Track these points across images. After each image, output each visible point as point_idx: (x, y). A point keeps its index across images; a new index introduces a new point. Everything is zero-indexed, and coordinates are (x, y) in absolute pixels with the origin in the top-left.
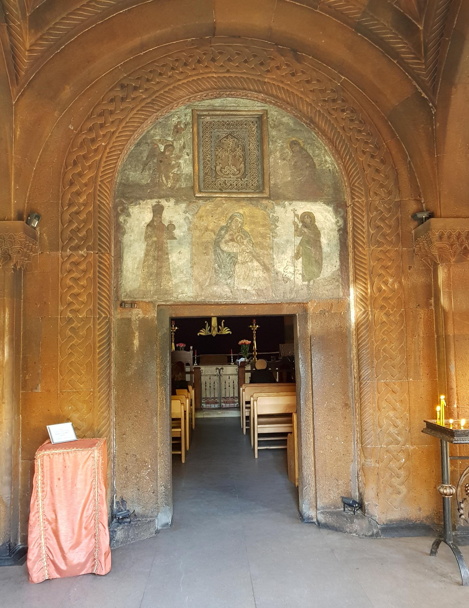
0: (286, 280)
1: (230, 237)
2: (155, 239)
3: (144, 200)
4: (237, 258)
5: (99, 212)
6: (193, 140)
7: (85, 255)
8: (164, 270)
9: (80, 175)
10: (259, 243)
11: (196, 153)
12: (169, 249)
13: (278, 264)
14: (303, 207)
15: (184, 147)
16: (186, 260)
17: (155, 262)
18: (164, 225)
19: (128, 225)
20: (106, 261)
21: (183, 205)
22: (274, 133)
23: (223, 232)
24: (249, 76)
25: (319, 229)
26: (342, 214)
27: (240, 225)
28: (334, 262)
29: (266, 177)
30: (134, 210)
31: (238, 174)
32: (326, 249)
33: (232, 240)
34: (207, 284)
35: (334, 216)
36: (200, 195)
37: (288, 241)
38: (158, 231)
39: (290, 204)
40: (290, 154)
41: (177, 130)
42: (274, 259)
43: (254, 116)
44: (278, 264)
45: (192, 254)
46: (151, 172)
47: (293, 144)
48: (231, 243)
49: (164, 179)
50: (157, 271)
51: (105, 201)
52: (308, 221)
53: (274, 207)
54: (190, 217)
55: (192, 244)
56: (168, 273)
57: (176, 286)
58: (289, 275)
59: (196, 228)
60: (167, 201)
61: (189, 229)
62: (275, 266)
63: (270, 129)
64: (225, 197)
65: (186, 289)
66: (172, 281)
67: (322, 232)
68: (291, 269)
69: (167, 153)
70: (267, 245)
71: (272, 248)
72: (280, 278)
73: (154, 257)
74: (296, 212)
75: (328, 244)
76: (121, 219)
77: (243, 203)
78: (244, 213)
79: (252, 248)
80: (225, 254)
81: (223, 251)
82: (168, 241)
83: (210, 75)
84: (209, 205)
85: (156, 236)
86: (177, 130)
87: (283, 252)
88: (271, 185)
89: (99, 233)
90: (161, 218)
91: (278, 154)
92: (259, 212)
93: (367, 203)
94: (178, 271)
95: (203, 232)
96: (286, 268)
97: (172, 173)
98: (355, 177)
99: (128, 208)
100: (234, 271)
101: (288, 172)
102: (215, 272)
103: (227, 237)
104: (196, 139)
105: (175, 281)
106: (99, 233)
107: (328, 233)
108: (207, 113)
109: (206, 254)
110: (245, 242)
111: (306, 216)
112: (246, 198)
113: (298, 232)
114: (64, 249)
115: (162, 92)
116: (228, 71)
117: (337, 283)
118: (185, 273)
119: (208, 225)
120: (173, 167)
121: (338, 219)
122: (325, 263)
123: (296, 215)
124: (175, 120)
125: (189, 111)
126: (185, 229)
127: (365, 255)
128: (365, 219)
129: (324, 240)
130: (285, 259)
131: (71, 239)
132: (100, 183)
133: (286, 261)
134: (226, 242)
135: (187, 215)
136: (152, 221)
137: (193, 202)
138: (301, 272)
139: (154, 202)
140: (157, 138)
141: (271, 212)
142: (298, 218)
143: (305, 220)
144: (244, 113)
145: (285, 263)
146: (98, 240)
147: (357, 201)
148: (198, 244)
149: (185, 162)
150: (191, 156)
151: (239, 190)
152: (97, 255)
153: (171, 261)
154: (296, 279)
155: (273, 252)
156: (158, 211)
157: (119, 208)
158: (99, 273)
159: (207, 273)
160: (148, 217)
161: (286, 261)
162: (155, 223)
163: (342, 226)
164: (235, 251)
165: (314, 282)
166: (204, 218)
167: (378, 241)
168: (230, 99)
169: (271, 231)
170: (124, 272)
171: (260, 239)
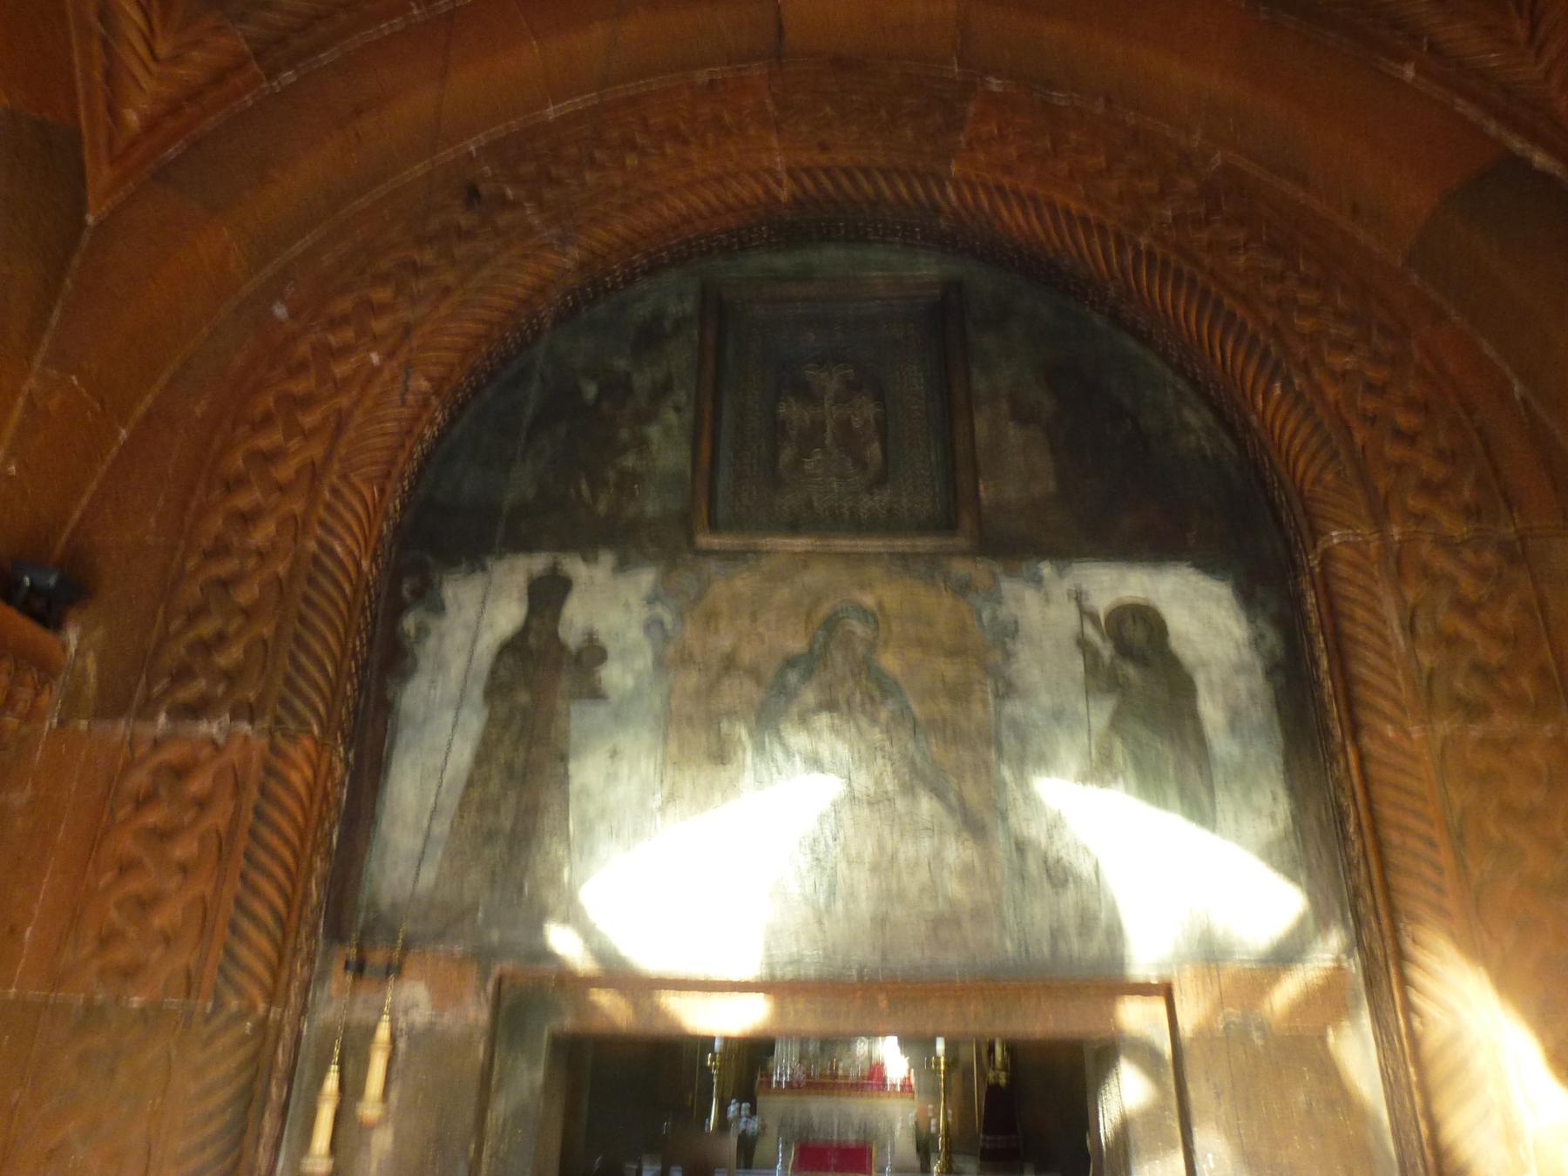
3: (500, 557)
5: (311, 581)
7: (221, 740)
9: (271, 457)
14: (1114, 585)
15: (663, 390)
18: (562, 647)
19: (431, 643)
21: (646, 578)
23: (793, 677)
30: (460, 593)
39: (1061, 575)
41: (650, 338)
49: (584, 487)
52: (1137, 634)
54: (668, 618)
59: (685, 659)
60: (585, 560)
61: (660, 663)
67: (1200, 680)
72: (1033, 867)
76: (409, 623)
77: (875, 572)
78: (880, 605)
82: (575, 709)
91: (1005, 407)
92: (939, 605)
113: (1100, 678)
114: (146, 712)
119: (735, 650)
123: (1087, 614)
131: (182, 675)
135: (659, 610)
136: (523, 633)
139: (539, 563)
146: (279, 681)
150: (689, 415)
151: (860, 526)
153: (574, 786)
160: (508, 615)
162: (532, 640)
170: (384, 825)
171: (945, 706)
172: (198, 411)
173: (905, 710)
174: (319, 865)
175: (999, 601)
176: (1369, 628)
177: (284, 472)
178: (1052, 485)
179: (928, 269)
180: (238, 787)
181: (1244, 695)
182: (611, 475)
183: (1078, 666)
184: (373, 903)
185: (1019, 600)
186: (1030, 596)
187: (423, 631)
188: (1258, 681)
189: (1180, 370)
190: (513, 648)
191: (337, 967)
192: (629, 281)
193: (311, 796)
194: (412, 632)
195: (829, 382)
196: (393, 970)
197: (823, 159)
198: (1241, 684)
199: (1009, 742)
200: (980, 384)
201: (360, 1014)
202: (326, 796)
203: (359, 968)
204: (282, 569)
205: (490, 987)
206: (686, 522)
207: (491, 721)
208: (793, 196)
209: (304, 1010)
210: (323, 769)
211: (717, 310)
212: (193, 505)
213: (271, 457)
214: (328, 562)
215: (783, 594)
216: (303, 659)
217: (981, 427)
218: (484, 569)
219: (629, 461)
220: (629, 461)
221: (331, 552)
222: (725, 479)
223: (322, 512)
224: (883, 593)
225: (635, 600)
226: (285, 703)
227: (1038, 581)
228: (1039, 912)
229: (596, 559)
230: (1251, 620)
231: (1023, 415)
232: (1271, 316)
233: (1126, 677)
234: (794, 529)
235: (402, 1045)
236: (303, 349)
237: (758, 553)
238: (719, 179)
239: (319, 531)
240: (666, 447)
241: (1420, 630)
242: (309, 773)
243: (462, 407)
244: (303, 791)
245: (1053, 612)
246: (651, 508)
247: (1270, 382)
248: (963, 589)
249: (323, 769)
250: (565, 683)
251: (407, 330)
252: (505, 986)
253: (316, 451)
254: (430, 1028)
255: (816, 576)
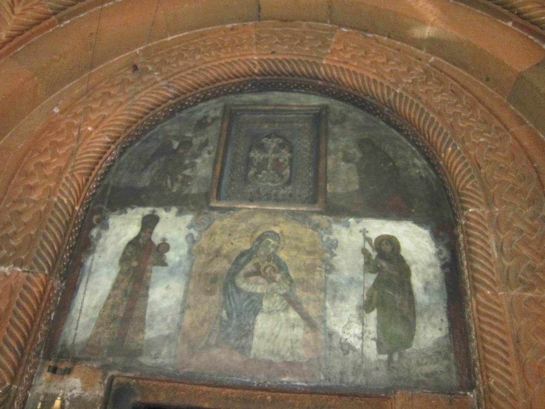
0: (346, 348)
1: (254, 269)
2: (135, 264)
4: (261, 303)
5: (53, 213)
6: (220, 136)
7: (8, 274)
8: (136, 313)
10: (301, 280)
11: (221, 152)
12: (153, 280)
13: (333, 319)
14: (379, 228)
15: (205, 144)
16: (175, 299)
17: (125, 299)
18: (152, 243)
19: (101, 241)
20: (36, 286)
21: (189, 218)
22: (336, 130)
24: (301, 58)
25: (408, 263)
26: (446, 241)
27: (272, 250)
28: (436, 321)
29: (321, 184)
31: (279, 182)
32: (421, 297)
33: (257, 273)
34: (203, 343)
35: (433, 244)
36: (218, 205)
37: (351, 280)
38: (144, 254)
39: (358, 222)
40: (359, 155)
41: (202, 125)
42: (324, 309)
43: (309, 112)
44: (333, 319)
45: (186, 292)
46: (153, 172)
47: (362, 144)
48: (253, 279)
49: (169, 182)
50: (125, 314)
51: (66, 197)
52: (388, 248)
53: (330, 226)
54: (196, 234)
55: (189, 275)
56: (142, 319)
57: (151, 344)
58: (353, 341)
60: (166, 210)
61: (190, 252)
62: (328, 323)
63: (330, 126)
64: (254, 209)
65: (165, 351)
66: (143, 333)
67: (413, 268)
68: (357, 329)
69: (181, 151)
70: (315, 284)
71: (324, 290)
72: (335, 343)
73: (126, 291)
74: (368, 235)
75: (425, 289)
76: (94, 232)
77: (281, 219)
78: (282, 232)
79: (288, 288)
80: (242, 295)
81: (239, 291)
82: (155, 268)
83: (250, 57)
84: (227, 218)
85: (137, 260)
86: (202, 125)
87: (343, 299)
88: (328, 195)
89: (41, 242)
90: (151, 233)
91: (340, 154)
92: (306, 234)
93: (491, 215)
94: (159, 318)
95: (211, 258)
96: (348, 326)
97: (182, 175)
98: (464, 176)
99: (108, 218)
100: (253, 324)
101: (355, 178)
102: (220, 324)
103: (249, 267)
104: (224, 136)
105: (150, 334)
106: (41, 242)
107: (424, 269)
108: (245, 107)
109: (211, 292)
110: (278, 277)
111: (384, 242)
112: (287, 210)
113: (370, 265)
115: (183, 74)
116: (273, 53)
117: (446, 362)
118: (169, 320)
119: (221, 247)
120: (186, 168)
121: (440, 247)
122: (420, 324)
124: (200, 115)
125: (221, 105)
126: (184, 251)
127: (499, 306)
128: (492, 241)
129: (417, 282)
130: (347, 311)
132: (68, 175)
133: (349, 313)
134: (248, 275)
135: (192, 231)
137: (205, 213)
138: (374, 335)
139: (147, 211)
140: (173, 133)
141: (325, 233)
142: (371, 244)
143: (383, 248)
144: (295, 108)
145: (345, 317)
147: (472, 212)
148: (200, 275)
149: (204, 161)
150: (213, 155)
151: (277, 200)
152: (26, 274)
154: (365, 348)
155: (325, 296)
156: (149, 222)
157: (95, 217)
158: (18, 304)
159: (206, 325)
161: (349, 313)
162: (141, 241)
163: (447, 260)
164: (259, 291)
165: (401, 356)
166: (217, 237)
167: (521, 281)
168: (277, 93)
169: (323, 260)
172: (20, 147)
173: (288, 275)
174: (44, 327)
175: (331, 233)
176: (482, 248)
177: (48, 172)
178: (357, 187)
179: (315, 101)
180: (12, 293)
181: (432, 277)
182: (180, 177)
183: (362, 261)
184: (64, 345)
185: (339, 233)
186: (344, 230)
187: (99, 236)
188: (438, 270)
189: (413, 142)
190: (133, 243)
191: (46, 369)
192: (196, 103)
193: (42, 299)
194: (95, 236)
195: (272, 144)
196: (68, 372)
197: (272, 57)
198: (431, 271)
199: (330, 291)
200: (331, 146)
201: (53, 390)
202: (49, 299)
203: (54, 370)
204: (42, 208)
205: (106, 381)
206: (207, 196)
207: (121, 272)
208: (260, 71)
209: (30, 387)
210: (49, 287)
211: (231, 115)
212: (13, 183)
213: (47, 164)
214: (60, 205)
215: (243, 226)
216: (45, 243)
217: (330, 162)
218: (126, 212)
219: (187, 172)
220: (187, 172)
221: (62, 201)
222: (225, 180)
223: (61, 187)
224: (284, 228)
225: (183, 226)
226: (35, 261)
227: (348, 226)
228: (337, 365)
229: (170, 210)
230: (437, 246)
231: (347, 159)
232: (449, 121)
233: (382, 266)
234: (251, 201)
235: (67, 403)
236: (63, 126)
237: (233, 209)
238: (230, 64)
239: (59, 194)
240: (203, 167)
241: (505, 249)
242: (41, 289)
243: (124, 149)
244: (37, 295)
245: (353, 238)
246: (194, 191)
247: (447, 146)
248: (316, 227)
249: (49, 287)
250: (152, 259)
251: (104, 118)
252: (115, 382)
253: (63, 165)
254: (79, 398)
255: (257, 220)
